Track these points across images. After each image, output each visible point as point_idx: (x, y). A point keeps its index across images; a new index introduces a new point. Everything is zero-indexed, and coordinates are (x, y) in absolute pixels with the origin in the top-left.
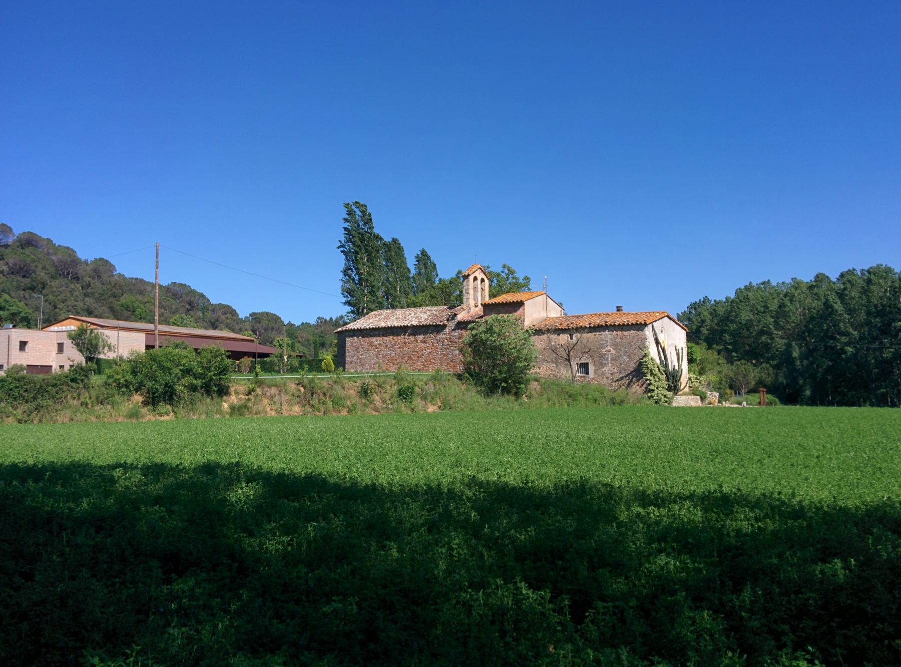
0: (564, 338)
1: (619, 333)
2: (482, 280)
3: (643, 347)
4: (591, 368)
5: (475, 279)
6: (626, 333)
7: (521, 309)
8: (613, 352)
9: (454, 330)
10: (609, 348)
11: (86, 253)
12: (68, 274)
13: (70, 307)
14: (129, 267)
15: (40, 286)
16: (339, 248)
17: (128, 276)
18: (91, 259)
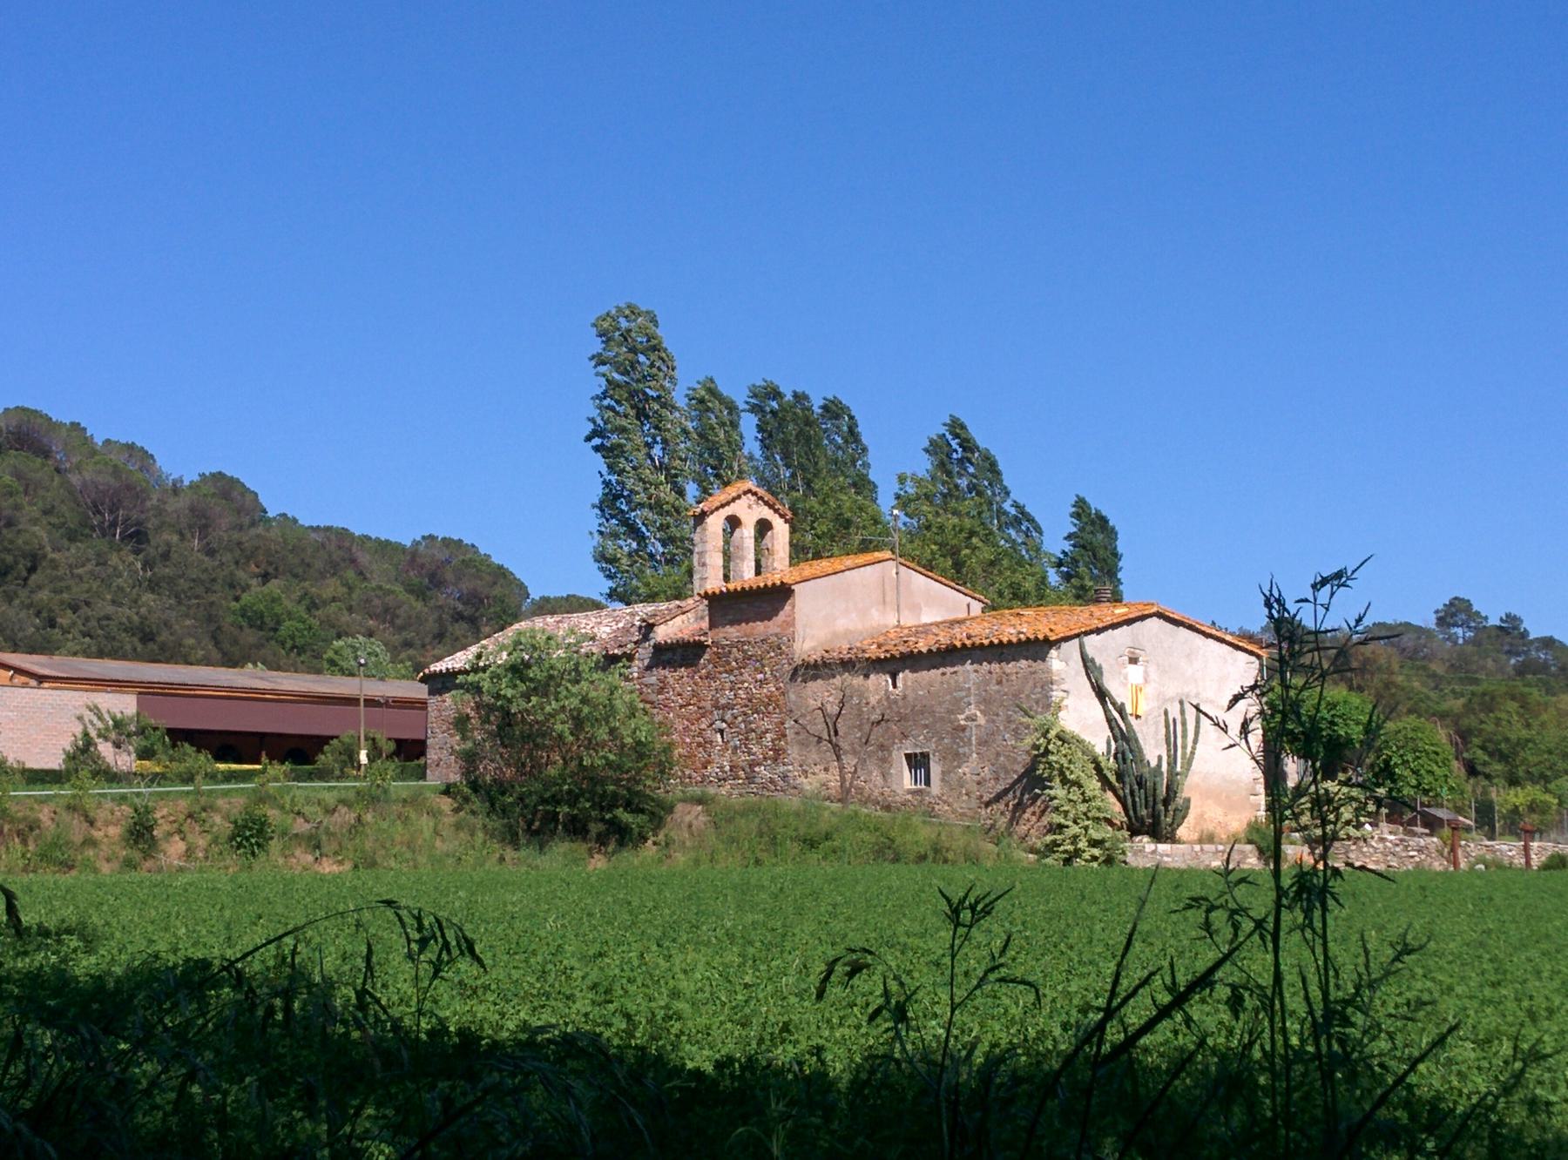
0: (879, 683)
1: (995, 667)
2: (763, 527)
3: (1043, 697)
4: (936, 769)
5: (734, 522)
6: (1010, 667)
7: (787, 607)
8: (982, 720)
9: (649, 668)
10: (973, 710)
11: (181, 461)
12: (114, 524)
13: (93, 623)
14: (302, 490)
15: (22, 568)
16: (588, 439)
17: (305, 521)
18: (190, 476)
